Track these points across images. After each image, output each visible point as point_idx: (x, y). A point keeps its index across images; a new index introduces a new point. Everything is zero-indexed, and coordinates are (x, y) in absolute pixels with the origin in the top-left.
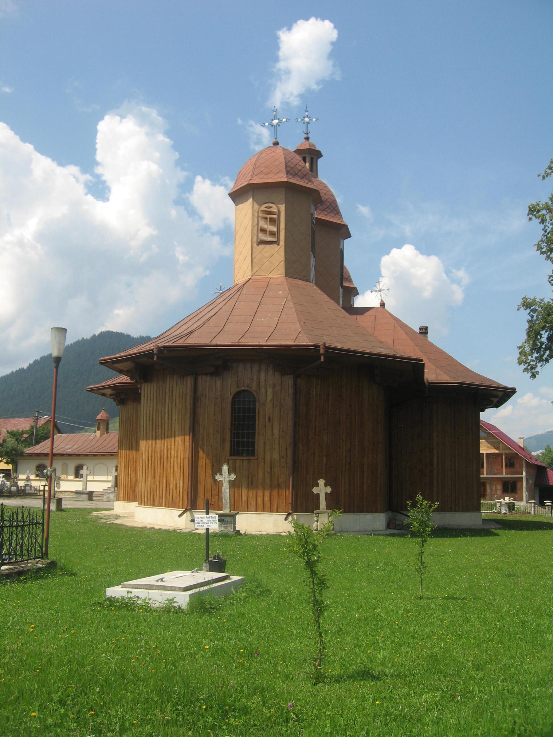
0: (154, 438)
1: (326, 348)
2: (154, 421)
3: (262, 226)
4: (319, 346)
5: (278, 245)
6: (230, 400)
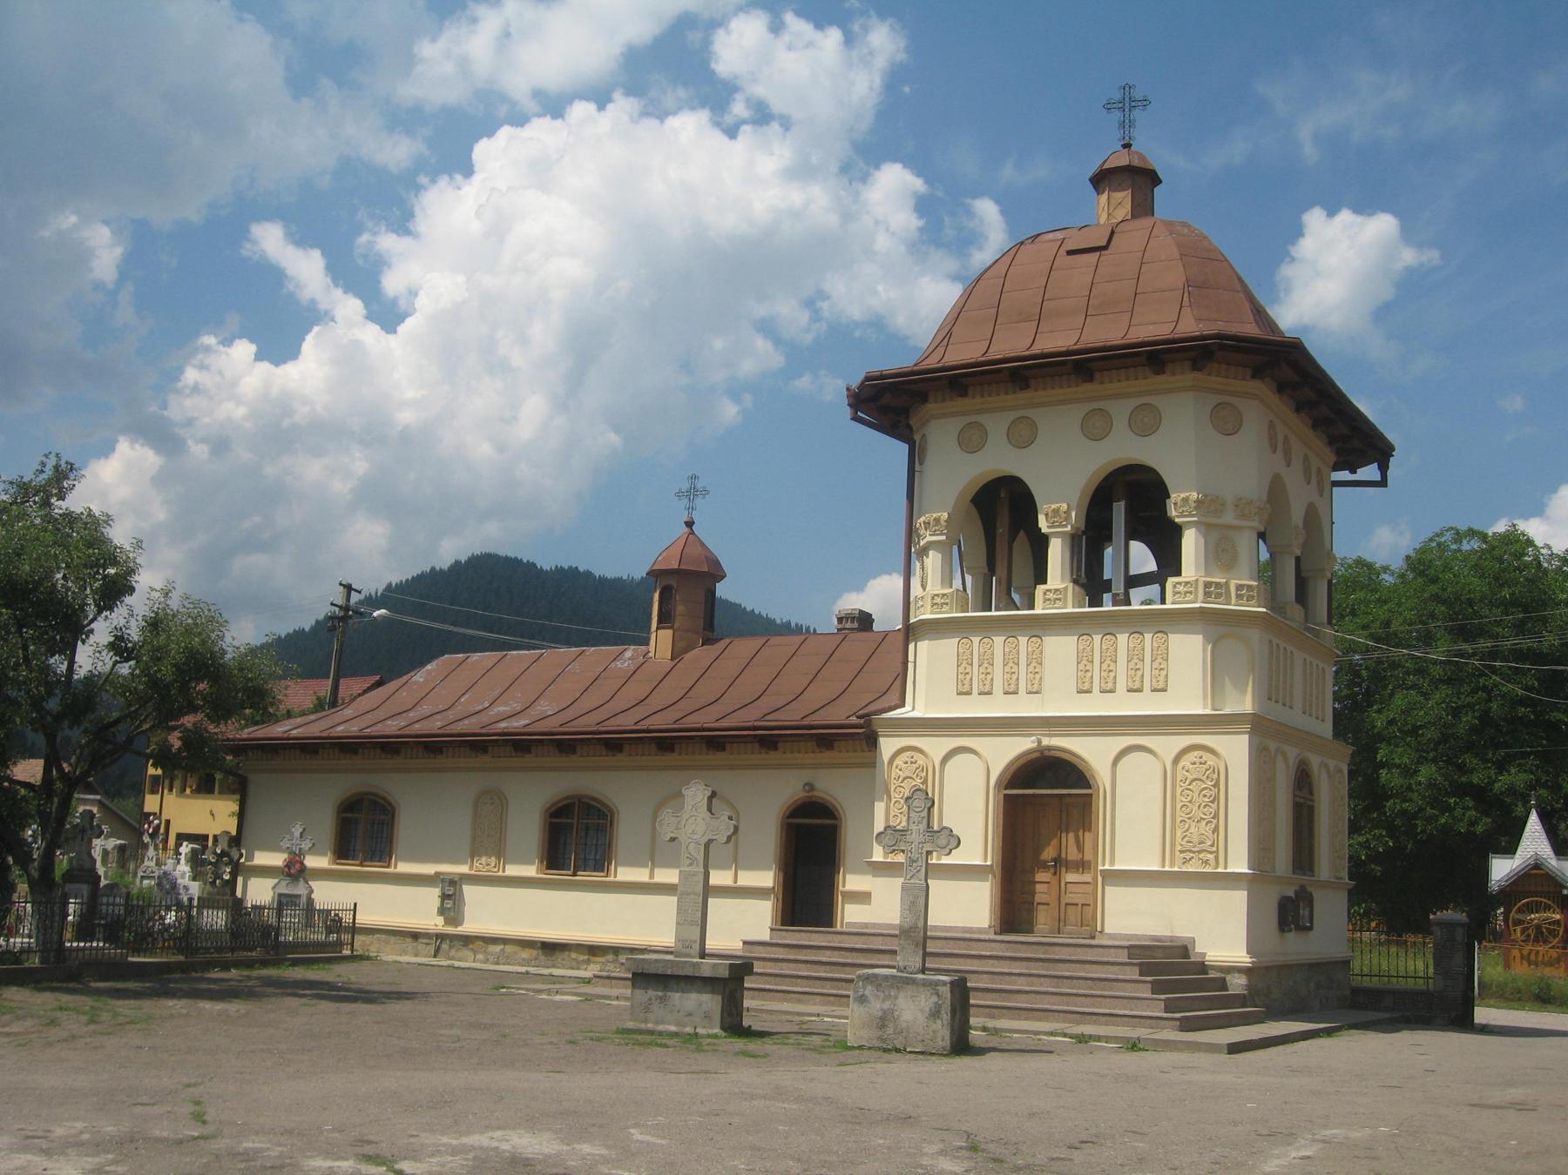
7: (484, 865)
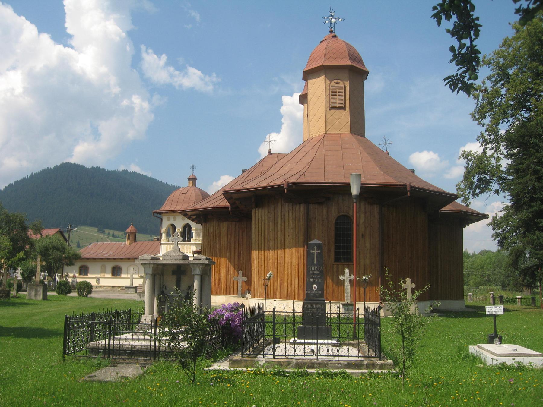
0: (266, 248)
1: (412, 187)
2: (266, 237)
3: (332, 96)
4: (406, 185)
5: (345, 110)
6: (334, 222)
7: (103, 275)
